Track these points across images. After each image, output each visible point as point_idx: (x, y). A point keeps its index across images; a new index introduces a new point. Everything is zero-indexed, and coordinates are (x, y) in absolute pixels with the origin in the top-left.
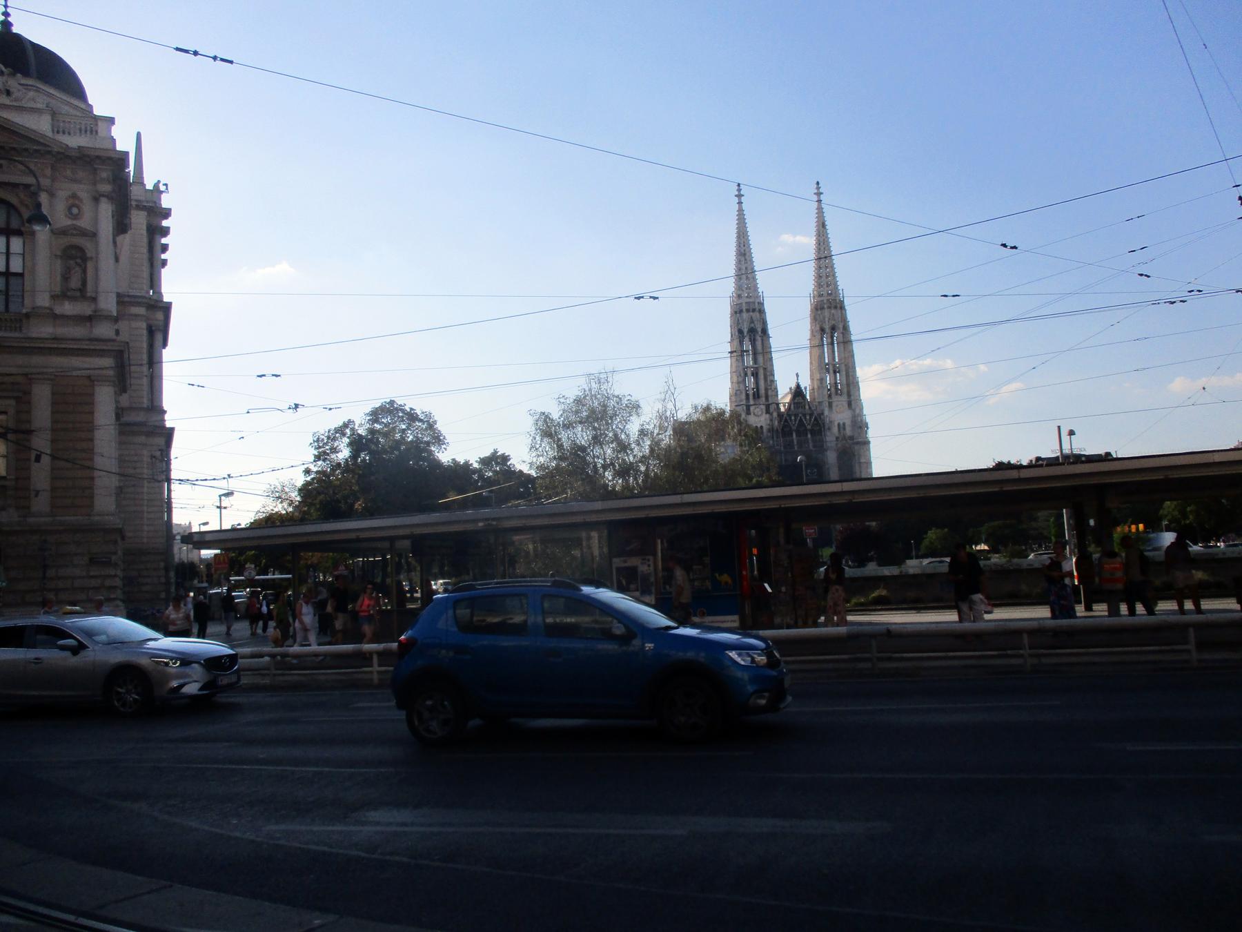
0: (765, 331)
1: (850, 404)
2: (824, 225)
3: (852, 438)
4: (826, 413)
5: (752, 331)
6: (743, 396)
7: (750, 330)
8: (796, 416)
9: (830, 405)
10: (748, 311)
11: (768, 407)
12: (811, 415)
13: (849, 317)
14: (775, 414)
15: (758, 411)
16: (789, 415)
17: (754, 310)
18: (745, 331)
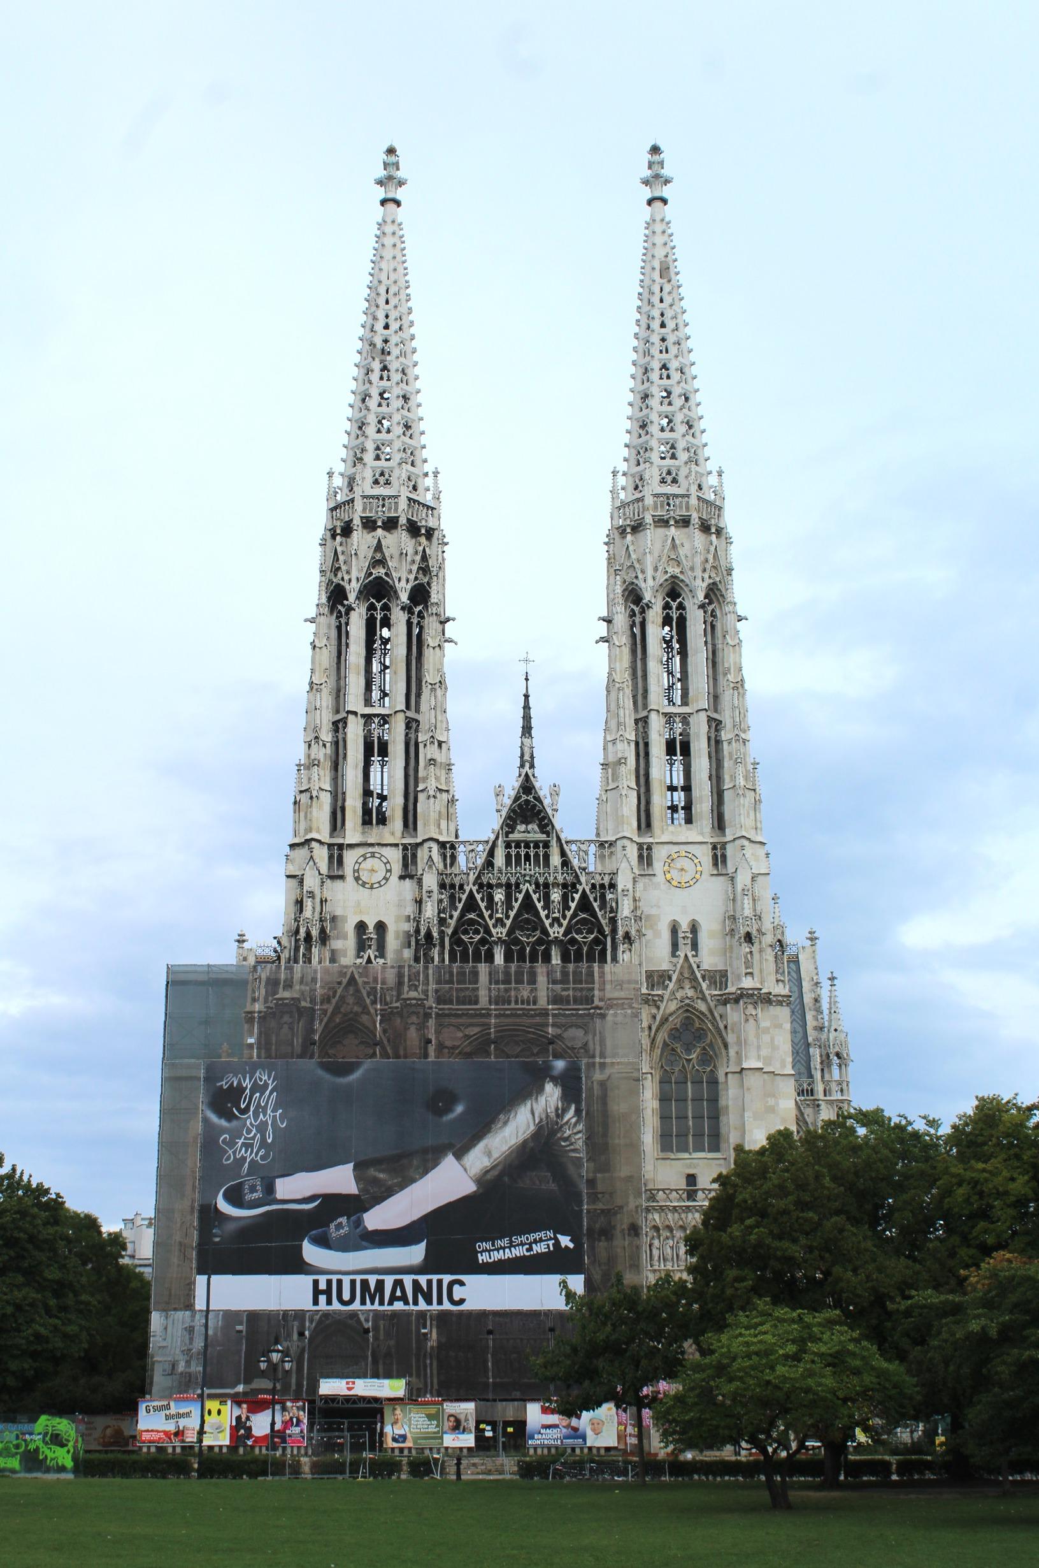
0: (420, 595)
1: (719, 858)
2: (665, 271)
3: (719, 978)
4: (623, 881)
5: (378, 590)
6: (322, 813)
7: (382, 589)
8: (510, 888)
9: (645, 855)
10: (369, 524)
11: (409, 855)
12: (569, 888)
13: (737, 554)
14: (430, 881)
15: (373, 869)
16: (486, 888)
17: (391, 524)
18: (353, 590)
